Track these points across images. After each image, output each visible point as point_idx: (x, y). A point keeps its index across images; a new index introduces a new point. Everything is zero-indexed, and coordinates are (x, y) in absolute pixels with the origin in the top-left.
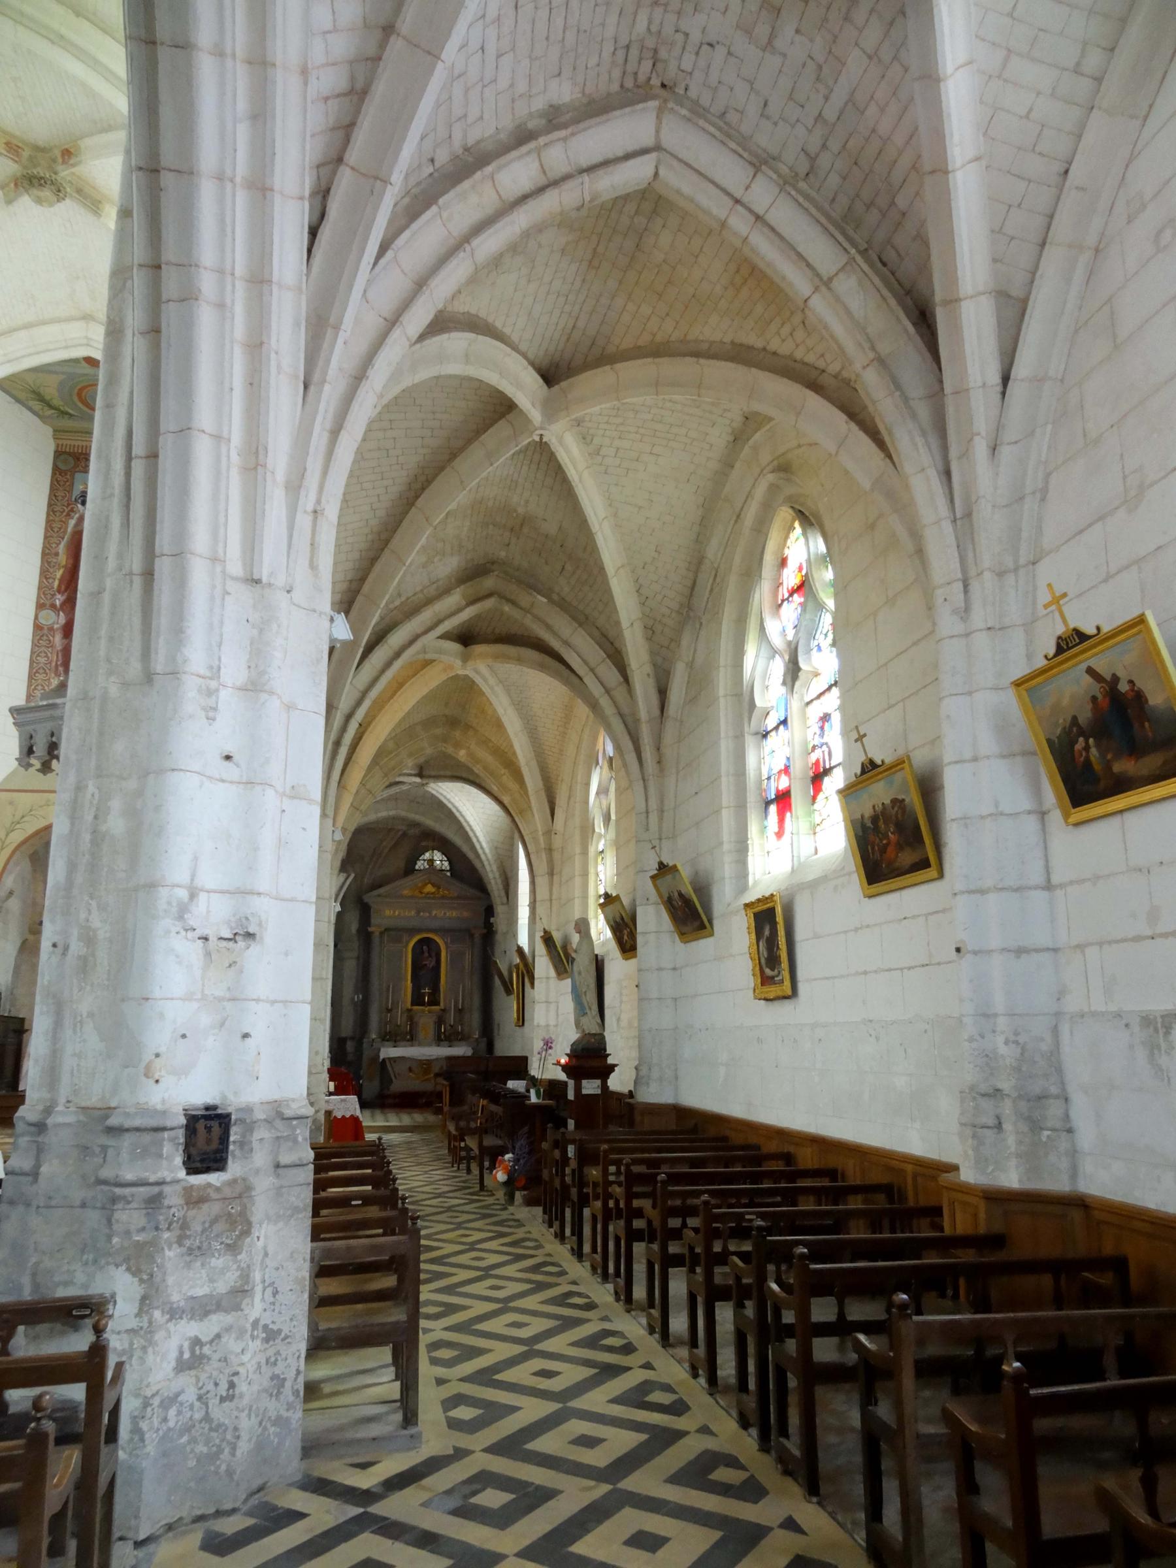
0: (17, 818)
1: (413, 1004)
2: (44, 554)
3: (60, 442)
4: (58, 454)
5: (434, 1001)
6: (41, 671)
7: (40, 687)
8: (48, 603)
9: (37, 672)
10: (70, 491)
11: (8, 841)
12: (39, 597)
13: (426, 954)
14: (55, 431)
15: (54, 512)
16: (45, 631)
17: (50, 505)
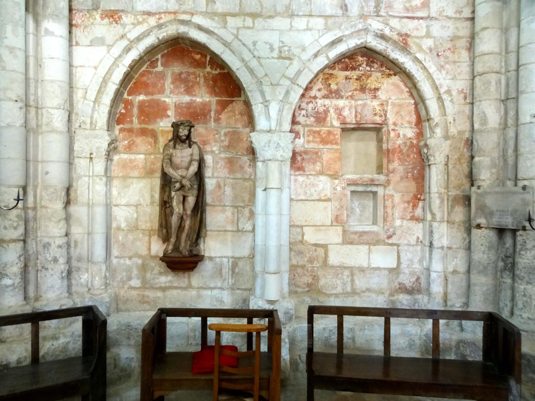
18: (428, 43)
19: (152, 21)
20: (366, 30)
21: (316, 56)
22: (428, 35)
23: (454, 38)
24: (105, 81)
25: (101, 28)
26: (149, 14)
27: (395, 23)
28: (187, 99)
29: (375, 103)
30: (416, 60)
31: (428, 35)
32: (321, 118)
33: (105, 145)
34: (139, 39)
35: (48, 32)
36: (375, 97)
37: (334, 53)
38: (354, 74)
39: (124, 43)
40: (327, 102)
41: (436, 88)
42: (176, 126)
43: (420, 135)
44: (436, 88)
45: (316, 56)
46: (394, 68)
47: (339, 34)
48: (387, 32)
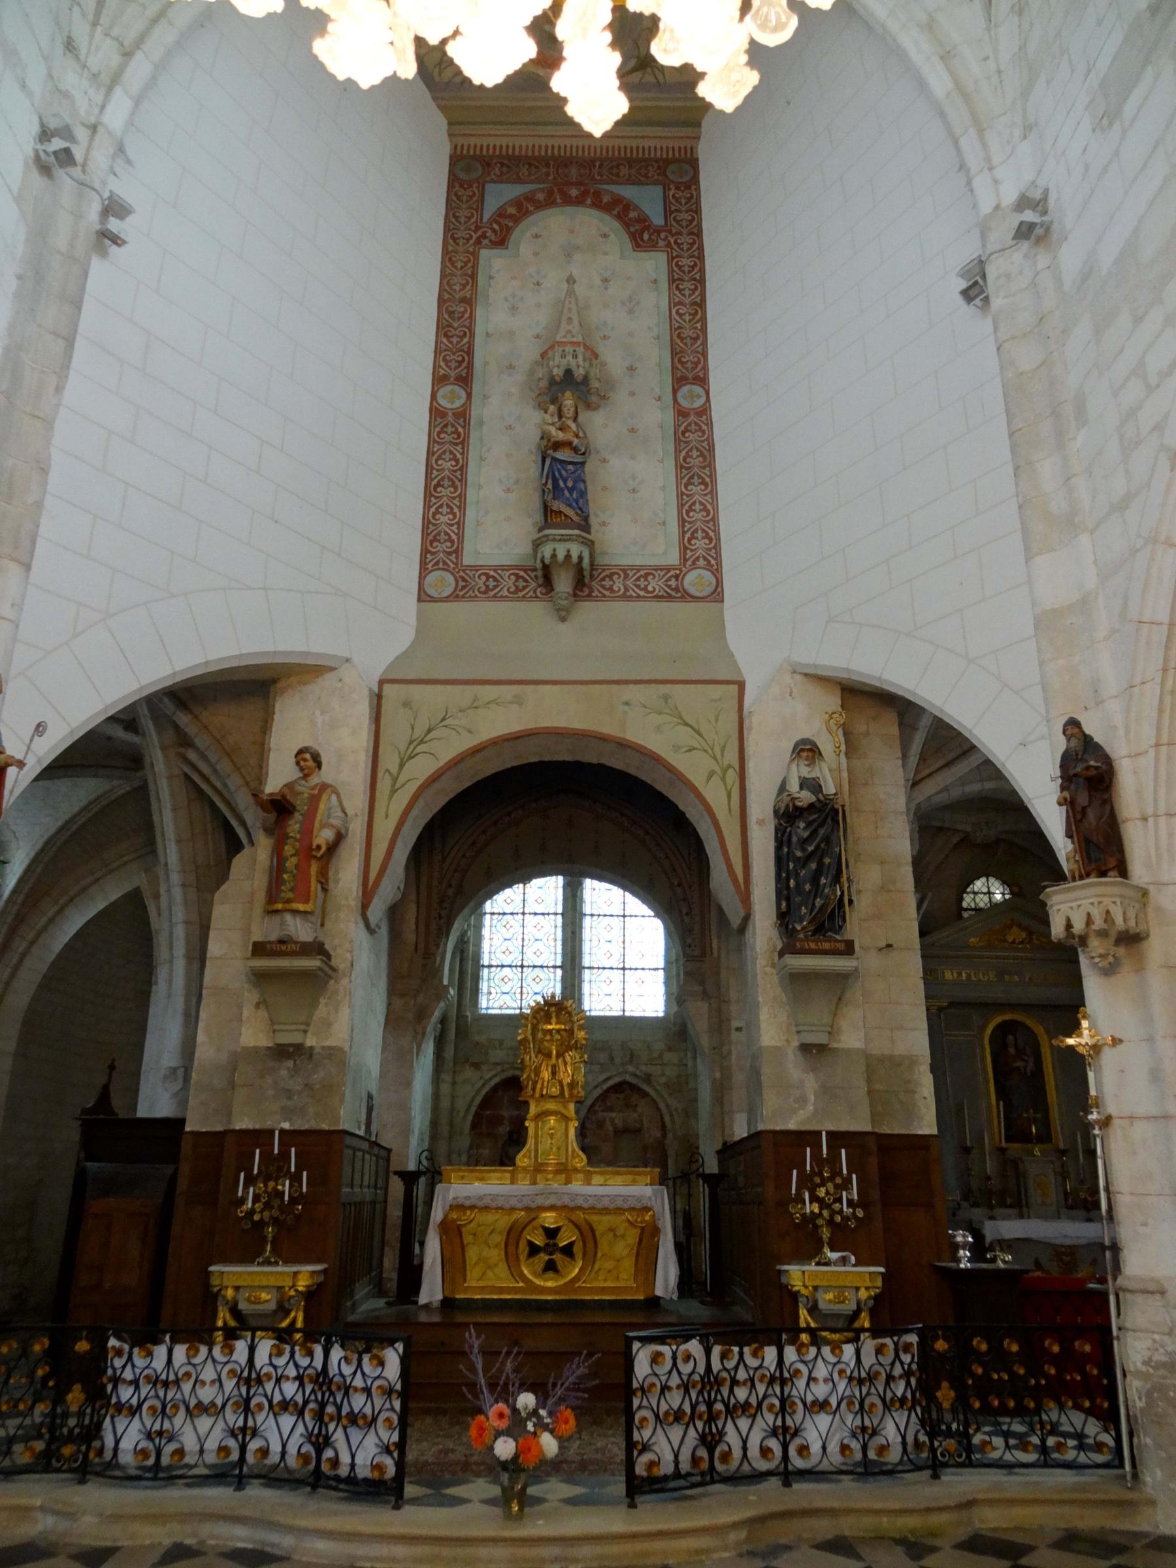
0: (419, 733)
1: (1008, 1140)
2: (441, 301)
3: (461, 141)
4: (455, 160)
5: (1045, 1137)
6: (446, 483)
7: (445, 510)
8: (453, 374)
9: (438, 485)
10: (480, 207)
11: (402, 779)
12: (436, 367)
13: (1012, 1051)
14: (450, 124)
15: (454, 239)
16: (450, 418)
17: (447, 229)
18: (663, 1080)
19: (499, 1068)
20: (626, 1072)
21: (596, 1087)
22: (663, 1074)
23: (679, 1076)
24: (469, 1106)
25: (468, 1073)
26: (498, 1064)
27: (643, 1068)
28: (516, 1113)
29: (635, 1115)
30: (656, 1090)
31: (663, 1074)
32: (600, 1125)
33: (467, 1145)
34: (491, 1079)
35: (443, 1081)
36: (635, 1111)
37: (605, 1087)
38: (621, 1096)
39: (482, 1082)
40: (605, 1114)
41: (667, 1105)
42: (510, 1133)
43: (664, 1136)
44: (667, 1105)
45: (596, 1087)
46: (644, 1094)
47: (609, 1074)
48: (638, 1072)
